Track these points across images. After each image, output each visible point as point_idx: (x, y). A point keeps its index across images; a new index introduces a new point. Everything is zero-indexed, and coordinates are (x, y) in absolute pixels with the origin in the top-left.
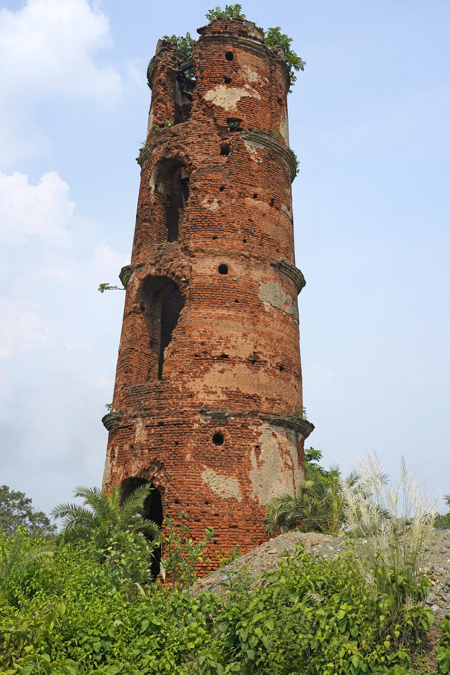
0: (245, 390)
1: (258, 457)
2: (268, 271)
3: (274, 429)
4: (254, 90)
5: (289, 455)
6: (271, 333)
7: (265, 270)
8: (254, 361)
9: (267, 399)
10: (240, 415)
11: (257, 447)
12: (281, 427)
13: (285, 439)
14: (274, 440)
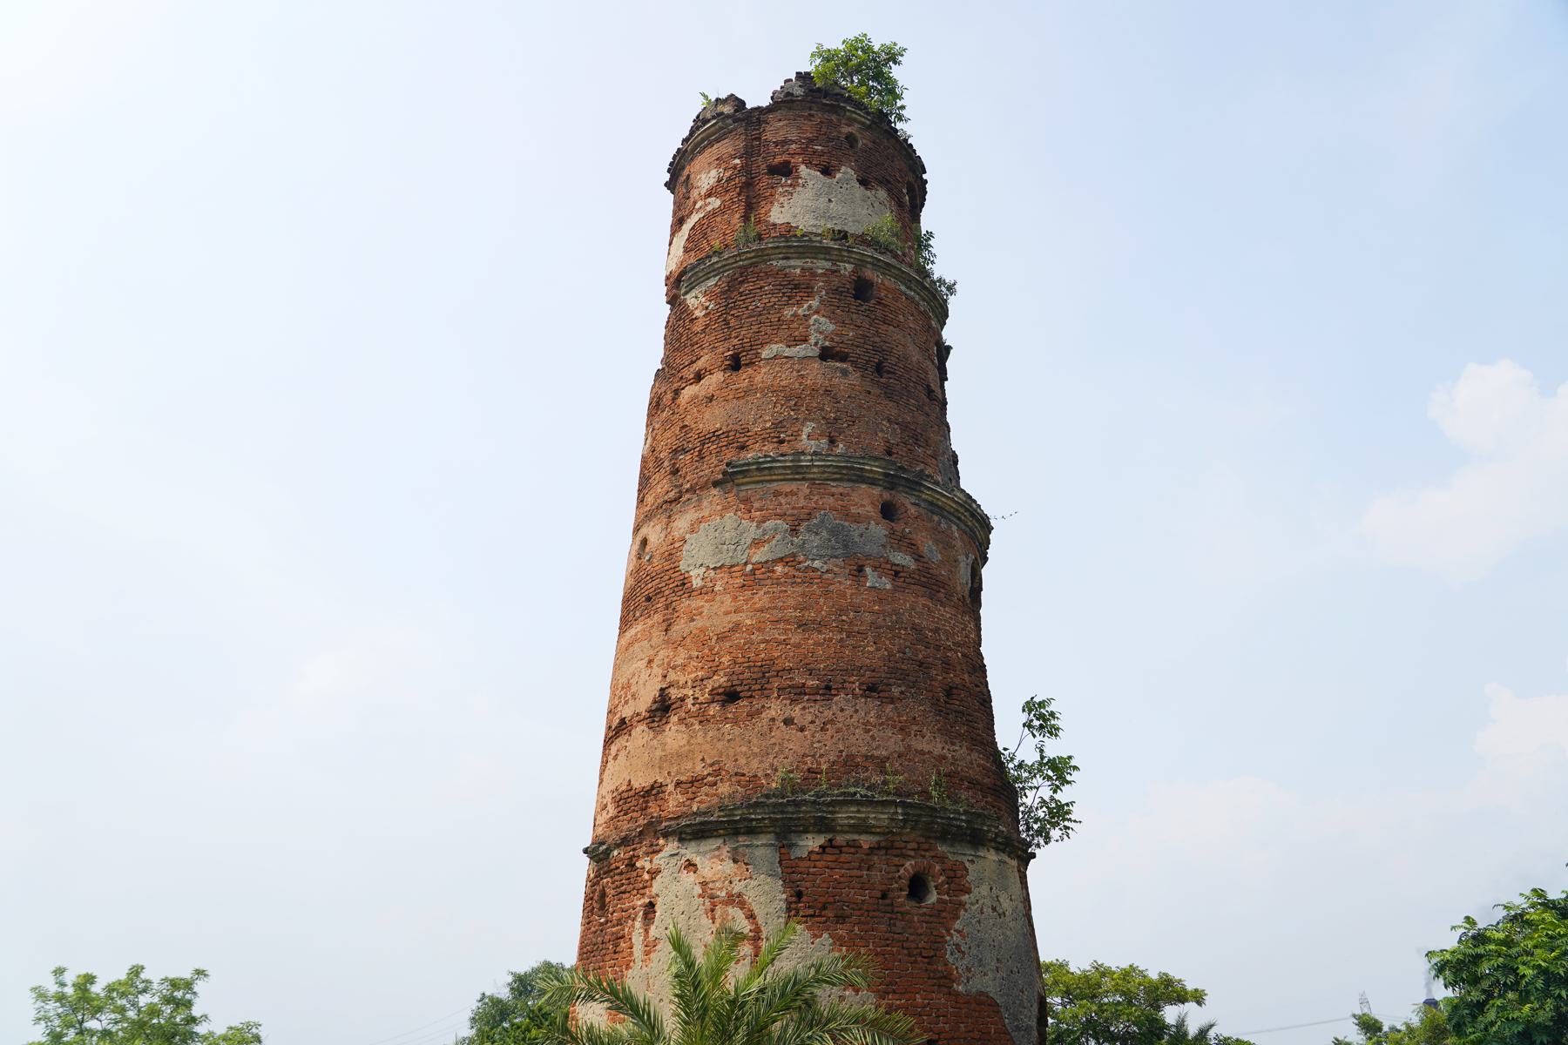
0: (641, 781)
1: (647, 931)
2: (705, 503)
3: (690, 852)
5: (742, 905)
6: (702, 630)
7: (699, 506)
8: (663, 708)
9: (678, 784)
11: (652, 905)
12: (711, 841)
13: (729, 867)
14: (689, 878)
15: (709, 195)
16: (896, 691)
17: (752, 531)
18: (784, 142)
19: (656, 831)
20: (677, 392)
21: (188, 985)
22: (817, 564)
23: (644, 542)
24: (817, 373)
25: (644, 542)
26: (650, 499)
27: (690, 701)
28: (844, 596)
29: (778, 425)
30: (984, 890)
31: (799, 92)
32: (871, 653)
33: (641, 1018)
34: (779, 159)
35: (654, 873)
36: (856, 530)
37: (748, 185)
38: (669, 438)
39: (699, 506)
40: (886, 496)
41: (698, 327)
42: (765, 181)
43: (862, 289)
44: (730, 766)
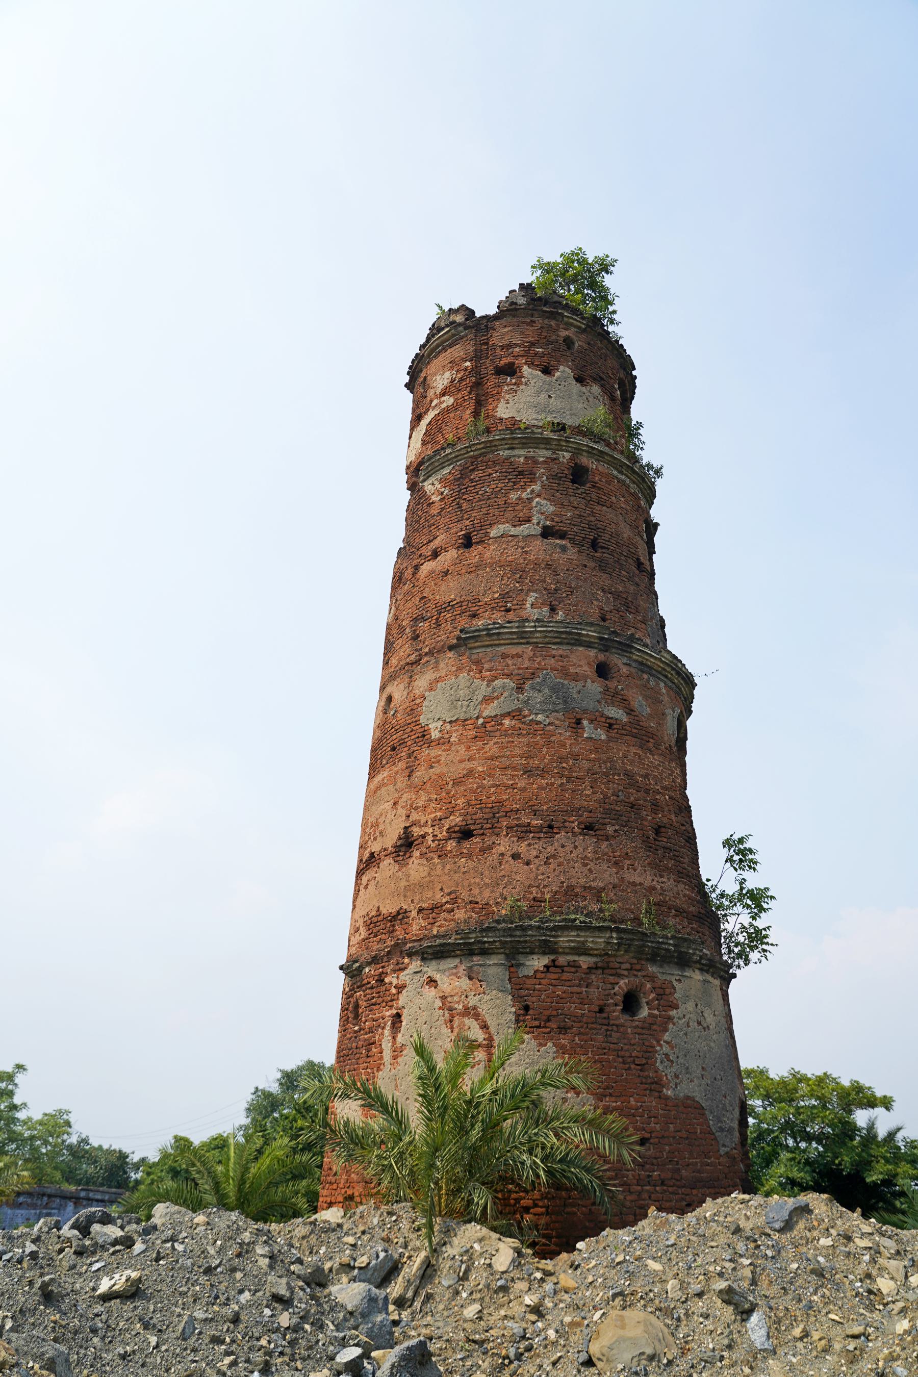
0: (388, 908)
1: (394, 1038)
2: (442, 665)
3: (431, 970)
4: (443, 398)
5: (477, 1016)
6: (440, 776)
7: (436, 667)
8: (407, 843)
9: (421, 910)
10: (375, 960)
11: (398, 1016)
12: (449, 960)
13: (464, 983)
14: (430, 993)
15: (443, 394)
16: (610, 829)
17: (483, 689)
18: (510, 346)
19: (401, 951)
20: (417, 568)
21: (10, 1078)
22: (540, 718)
23: (390, 699)
24: (539, 549)
25: (390, 699)
26: (394, 661)
27: (430, 838)
28: (563, 745)
29: (505, 596)
30: (690, 1006)
31: (522, 301)
32: (588, 796)
33: (390, 1115)
34: (504, 361)
35: (400, 988)
36: (574, 688)
37: (478, 384)
38: (411, 608)
39: (436, 667)
40: (601, 657)
41: (434, 511)
42: (492, 381)
43: (578, 475)
44: (465, 895)
